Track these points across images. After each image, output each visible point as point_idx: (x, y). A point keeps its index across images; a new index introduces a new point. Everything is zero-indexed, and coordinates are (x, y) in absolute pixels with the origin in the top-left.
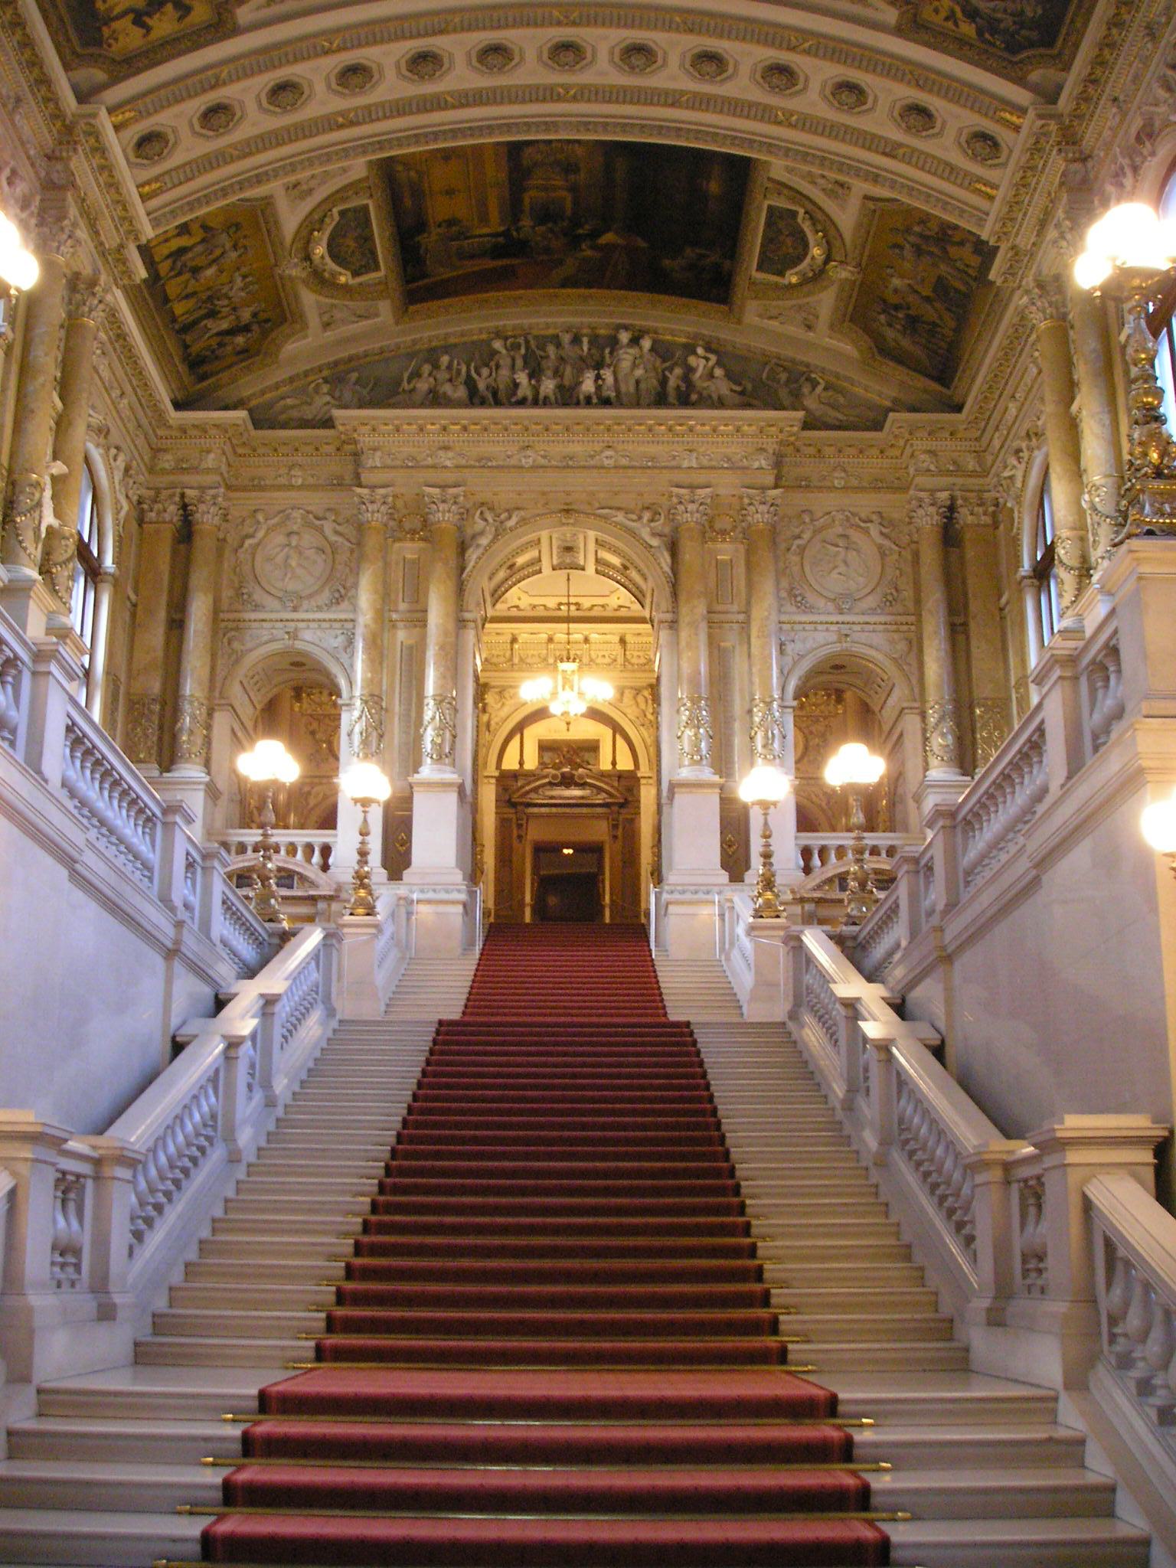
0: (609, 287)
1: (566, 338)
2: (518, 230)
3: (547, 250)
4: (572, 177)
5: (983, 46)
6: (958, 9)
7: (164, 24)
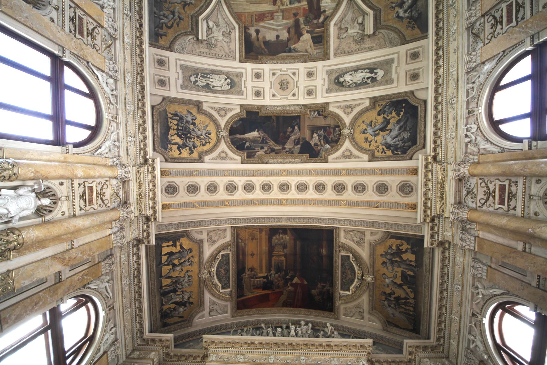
0: (296, 307)
1: (284, 326)
2: (270, 275)
3: (278, 287)
4: (285, 250)
5: (396, 156)
6: (384, 147)
7: (185, 153)
